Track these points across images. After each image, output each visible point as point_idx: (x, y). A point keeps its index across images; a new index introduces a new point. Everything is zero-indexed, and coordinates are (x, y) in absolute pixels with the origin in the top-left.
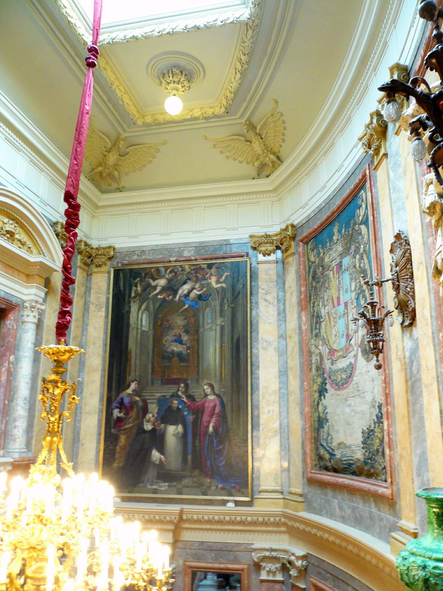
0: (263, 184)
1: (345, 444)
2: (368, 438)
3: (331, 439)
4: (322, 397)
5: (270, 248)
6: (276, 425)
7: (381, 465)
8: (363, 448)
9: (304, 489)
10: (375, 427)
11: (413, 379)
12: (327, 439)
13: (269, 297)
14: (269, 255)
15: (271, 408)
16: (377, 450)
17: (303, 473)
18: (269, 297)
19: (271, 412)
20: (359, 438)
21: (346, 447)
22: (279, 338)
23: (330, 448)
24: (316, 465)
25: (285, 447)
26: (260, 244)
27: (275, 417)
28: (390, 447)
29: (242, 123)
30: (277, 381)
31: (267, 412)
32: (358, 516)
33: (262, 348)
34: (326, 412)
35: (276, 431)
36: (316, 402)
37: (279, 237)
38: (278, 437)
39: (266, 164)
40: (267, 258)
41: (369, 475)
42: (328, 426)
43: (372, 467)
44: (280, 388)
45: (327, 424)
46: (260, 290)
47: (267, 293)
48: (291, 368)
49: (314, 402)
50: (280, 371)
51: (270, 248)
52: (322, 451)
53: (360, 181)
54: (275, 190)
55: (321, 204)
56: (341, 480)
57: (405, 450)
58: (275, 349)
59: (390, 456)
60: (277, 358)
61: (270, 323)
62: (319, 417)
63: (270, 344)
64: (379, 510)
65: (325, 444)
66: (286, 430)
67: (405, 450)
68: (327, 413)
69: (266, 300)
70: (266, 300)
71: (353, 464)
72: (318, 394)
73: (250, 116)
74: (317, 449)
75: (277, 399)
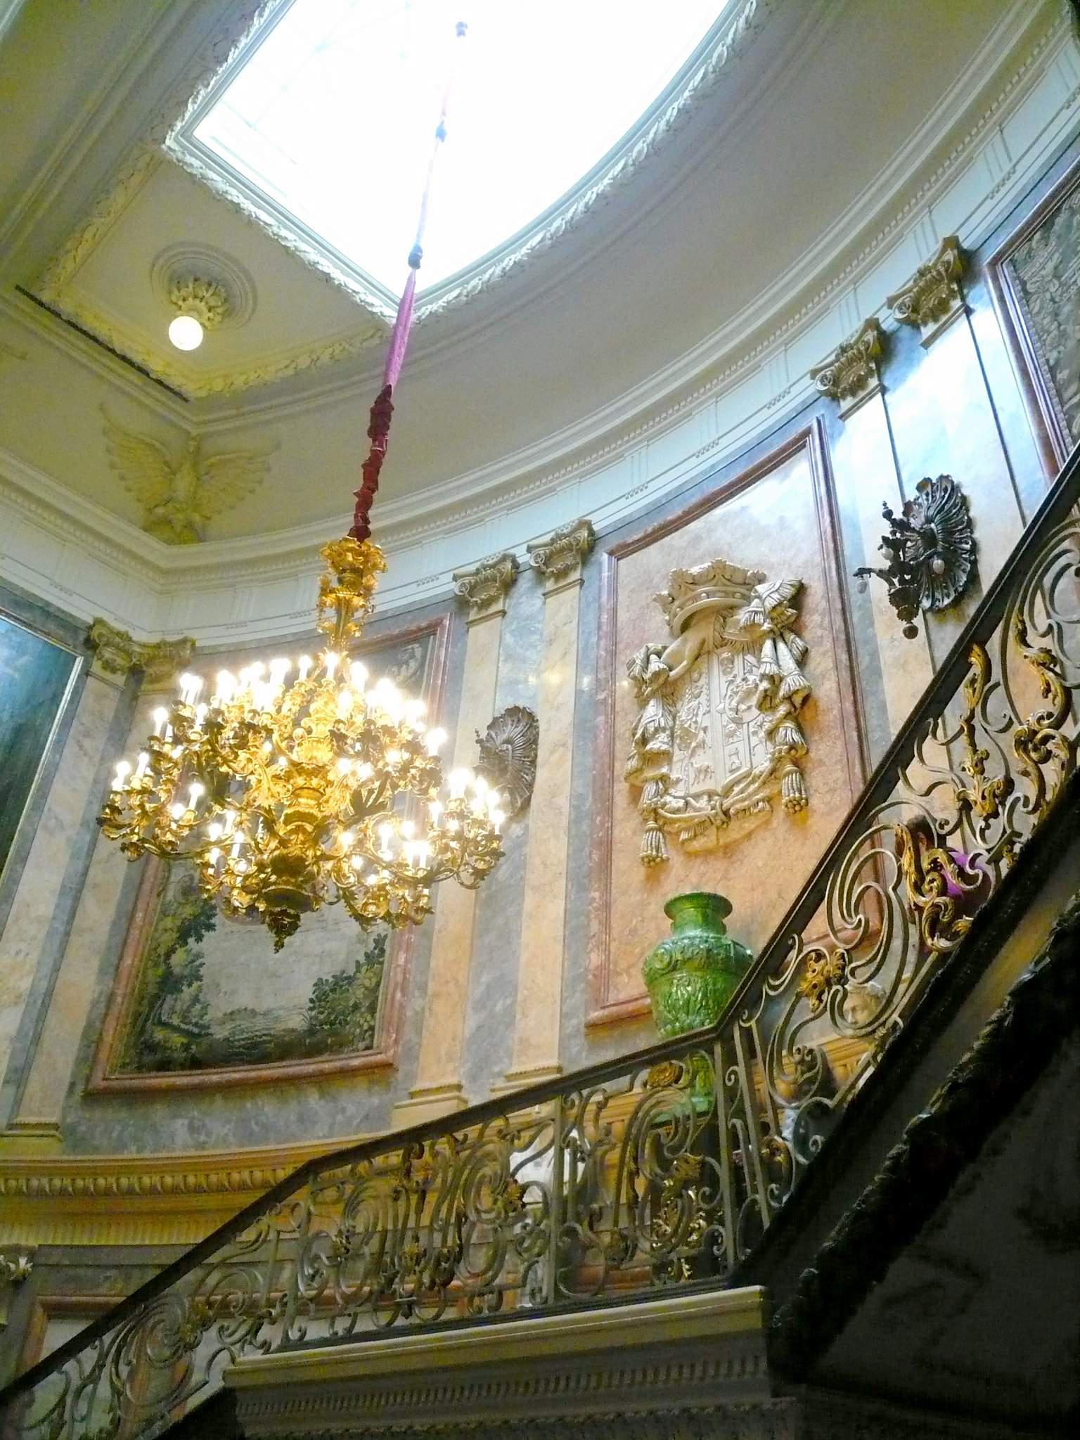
0: (154, 549)
1: (253, 1011)
2: (333, 990)
3: (205, 1008)
4: (191, 940)
5: (120, 661)
6: (25, 985)
7: (361, 1026)
8: (311, 1009)
9: (64, 1118)
10: (358, 971)
11: (494, 888)
12: (188, 1010)
13: (87, 743)
14: (114, 671)
15: (23, 946)
16: (356, 1007)
17: (73, 1085)
18: (87, 743)
19: (21, 957)
20: (306, 992)
21: (254, 1013)
22: (82, 825)
23: (196, 1025)
24: (124, 1065)
25: (27, 1034)
26: (106, 645)
27: (27, 967)
28: (404, 994)
29: (189, 433)
30: (54, 900)
31: (13, 952)
32: (256, 1129)
33: (46, 828)
34: (197, 963)
35: (20, 996)
36: (162, 951)
37: (150, 651)
38: (22, 1007)
39: (170, 522)
40: (108, 675)
41: (313, 1051)
42: (200, 987)
43: (334, 1033)
44: (54, 918)
45: (196, 984)
46: (75, 723)
47: (87, 734)
48: (95, 886)
49: (155, 949)
50: (63, 886)
51: (120, 661)
52: (159, 1035)
53: (420, 630)
54: (165, 573)
55: (285, 636)
56: (215, 1078)
57: (451, 985)
58: (69, 840)
59: (401, 1005)
60: (67, 858)
61: (74, 790)
62: (169, 973)
63: (61, 825)
64: (335, 1099)
65: (175, 1021)
66: (40, 1002)
67: (451, 985)
68: (202, 965)
69: (81, 747)
70: (81, 747)
71: (270, 1042)
72: (175, 935)
73: (211, 435)
74: (142, 1032)
75: (42, 936)
